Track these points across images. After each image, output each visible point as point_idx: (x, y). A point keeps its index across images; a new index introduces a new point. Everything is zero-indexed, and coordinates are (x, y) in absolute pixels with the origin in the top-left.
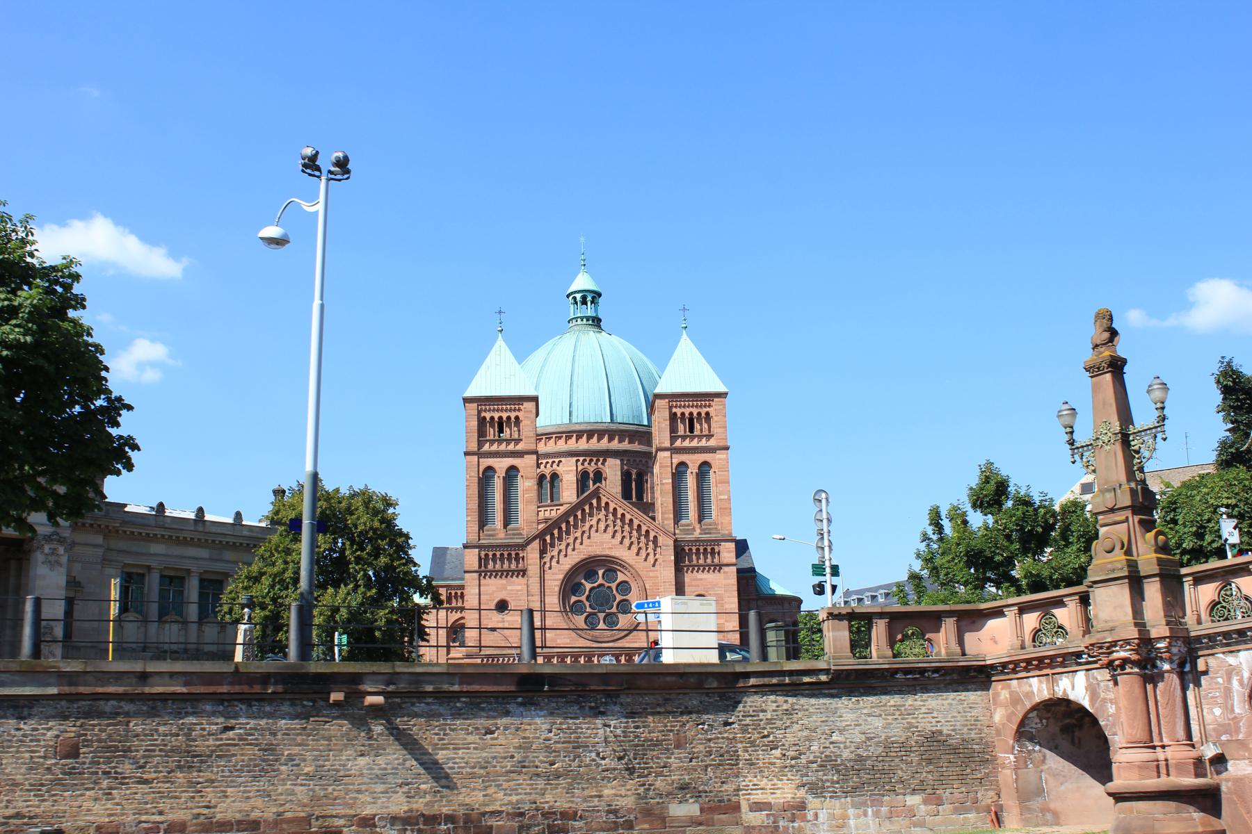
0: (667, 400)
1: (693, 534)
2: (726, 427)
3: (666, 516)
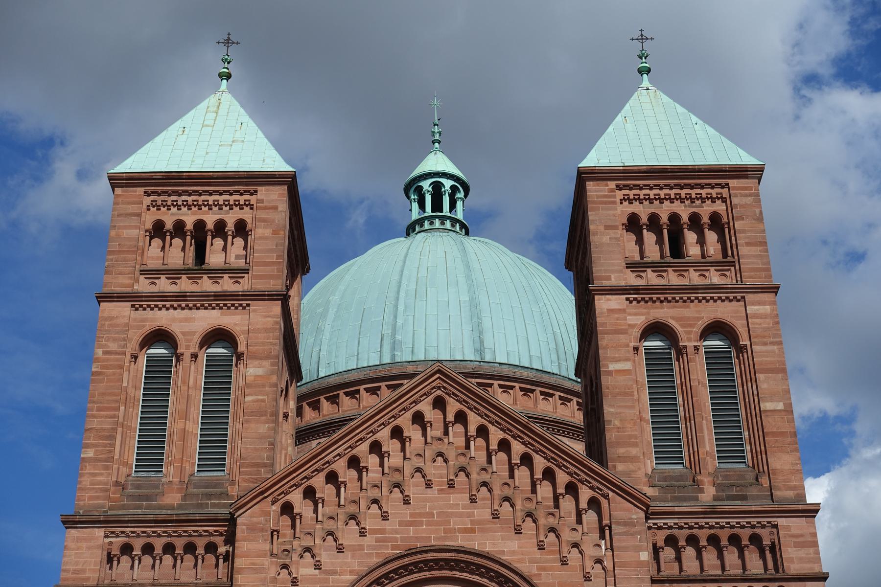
0: (612, 184)
3: (621, 451)
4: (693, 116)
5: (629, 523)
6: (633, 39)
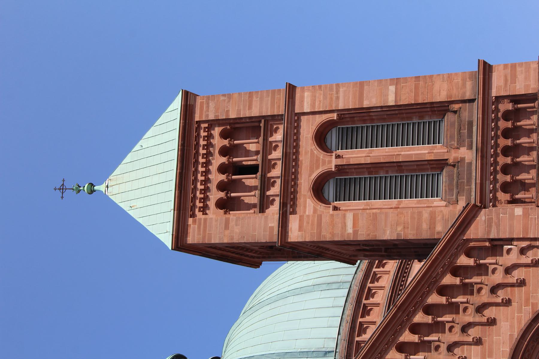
0: (190, 220)
1: (470, 164)
2: (251, 94)
4: (135, 149)
5: (489, 223)
6: (62, 197)
